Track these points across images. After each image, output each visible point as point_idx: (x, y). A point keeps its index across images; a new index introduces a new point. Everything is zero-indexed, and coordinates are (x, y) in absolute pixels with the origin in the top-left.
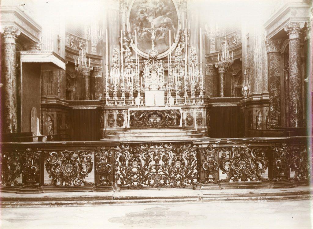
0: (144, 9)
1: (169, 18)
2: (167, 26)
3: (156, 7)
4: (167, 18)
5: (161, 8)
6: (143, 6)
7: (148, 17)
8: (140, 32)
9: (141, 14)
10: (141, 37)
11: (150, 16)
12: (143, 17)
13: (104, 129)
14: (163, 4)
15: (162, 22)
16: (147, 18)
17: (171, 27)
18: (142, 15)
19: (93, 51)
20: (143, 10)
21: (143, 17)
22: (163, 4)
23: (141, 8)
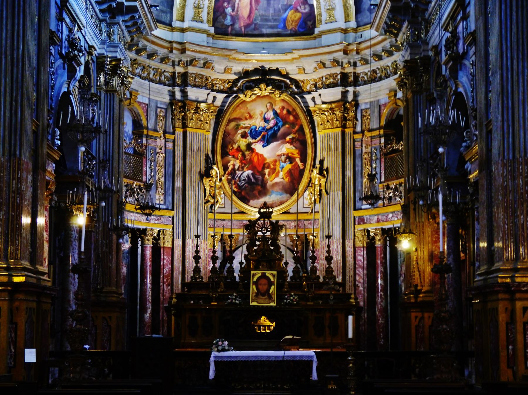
0: (247, 130)
1: (292, 146)
2: (287, 160)
3: (268, 127)
4: (288, 145)
5: (276, 129)
6: (246, 125)
7: (253, 144)
8: (241, 169)
9: (242, 139)
10: (242, 178)
11: (258, 141)
12: (246, 143)
13: (183, 341)
14: (280, 122)
15: (279, 153)
16: (253, 146)
17: (295, 160)
18: (244, 140)
19: (157, 202)
20: (245, 132)
21: (245, 144)
22: (280, 120)
23: (242, 128)
